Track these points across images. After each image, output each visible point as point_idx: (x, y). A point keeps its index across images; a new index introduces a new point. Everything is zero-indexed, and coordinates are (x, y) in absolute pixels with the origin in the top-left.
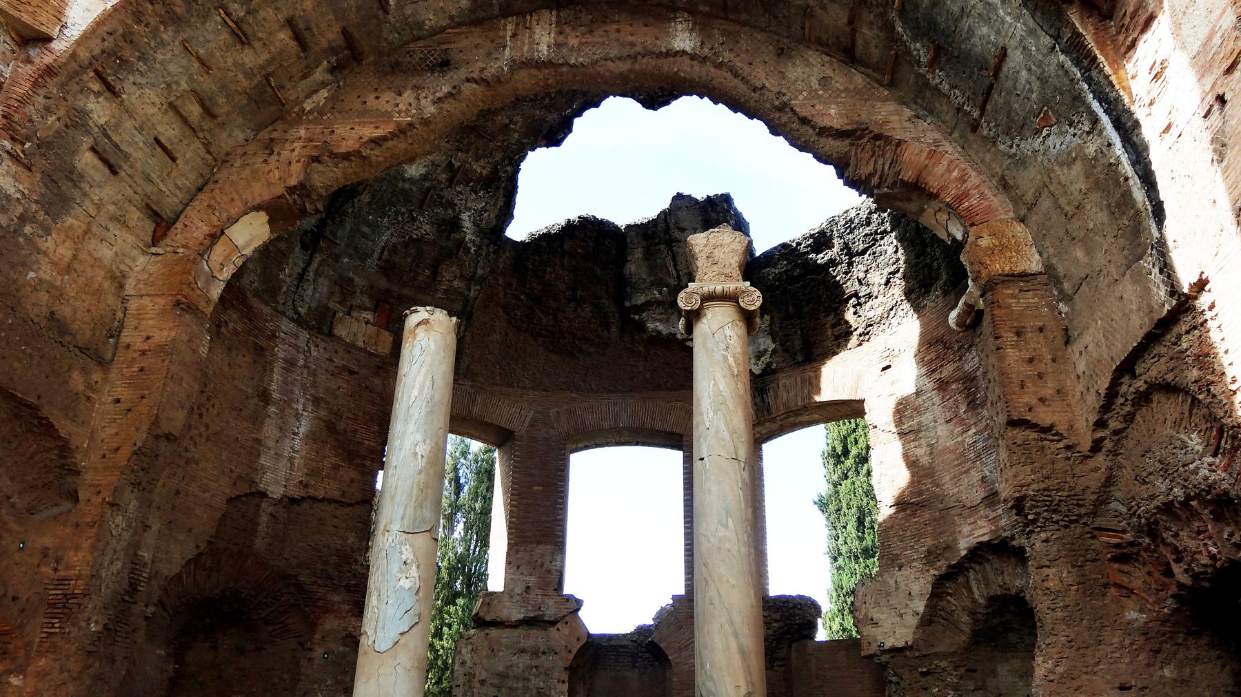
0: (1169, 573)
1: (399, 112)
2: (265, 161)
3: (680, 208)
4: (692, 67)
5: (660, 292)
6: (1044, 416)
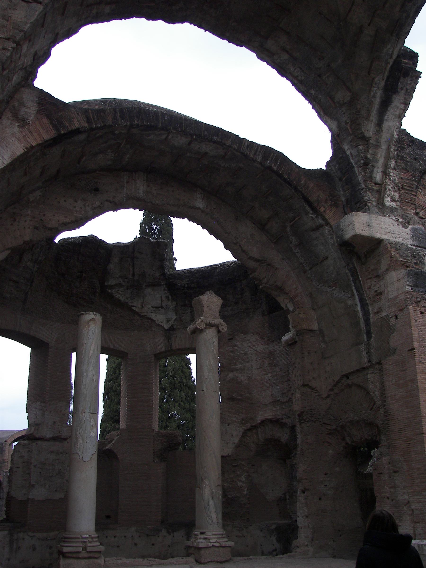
0: (344, 439)
1: (76, 211)
2: (12, 224)
5: (124, 281)
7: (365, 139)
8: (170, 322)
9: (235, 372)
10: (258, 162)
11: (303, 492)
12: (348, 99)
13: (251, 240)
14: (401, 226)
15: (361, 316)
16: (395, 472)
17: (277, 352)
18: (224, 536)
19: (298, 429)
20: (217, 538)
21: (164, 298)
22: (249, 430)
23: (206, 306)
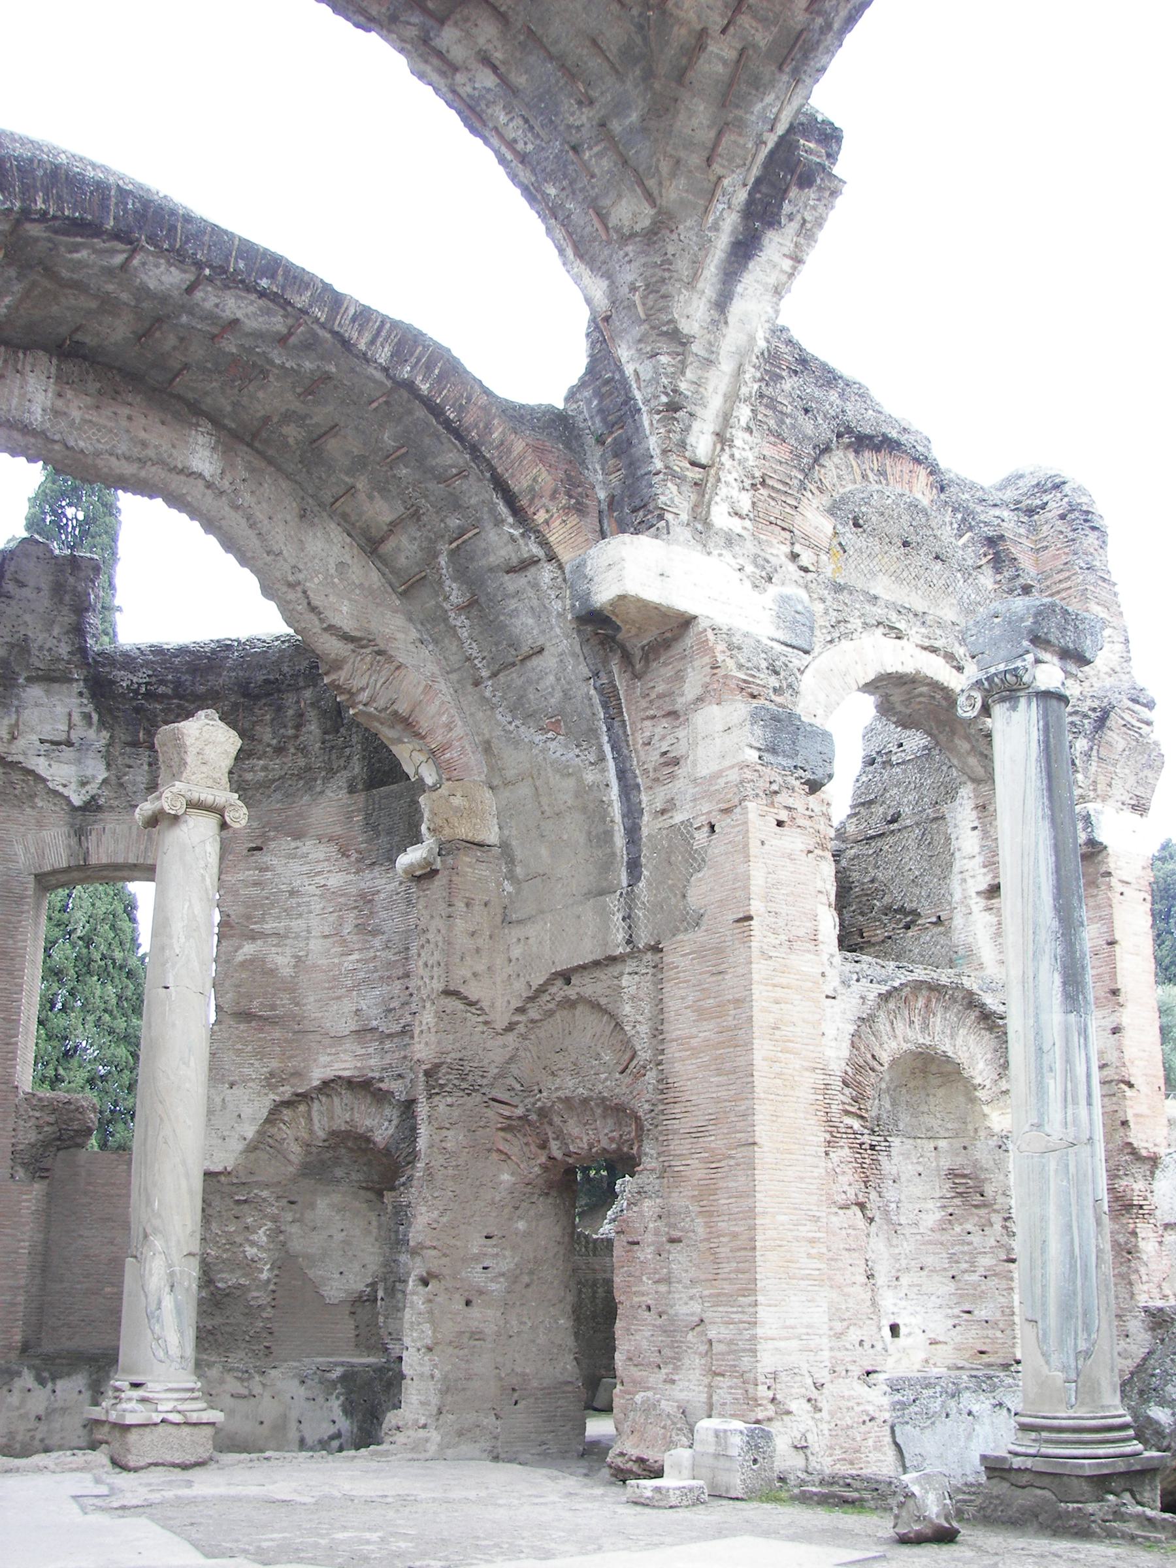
0: (544, 1146)
3: (27, 556)
4: (204, 495)
6: (473, 991)
7: (677, 339)
8: (88, 787)
9: (259, 942)
10: (380, 364)
11: (425, 1283)
12: (647, 222)
13: (336, 580)
14: (748, 584)
15: (618, 818)
16: (672, 1241)
17: (383, 896)
18: (196, 1394)
19: (422, 1109)
20: (177, 1400)
21: (76, 718)
22: (287, 1104)
23: (192, 751)
